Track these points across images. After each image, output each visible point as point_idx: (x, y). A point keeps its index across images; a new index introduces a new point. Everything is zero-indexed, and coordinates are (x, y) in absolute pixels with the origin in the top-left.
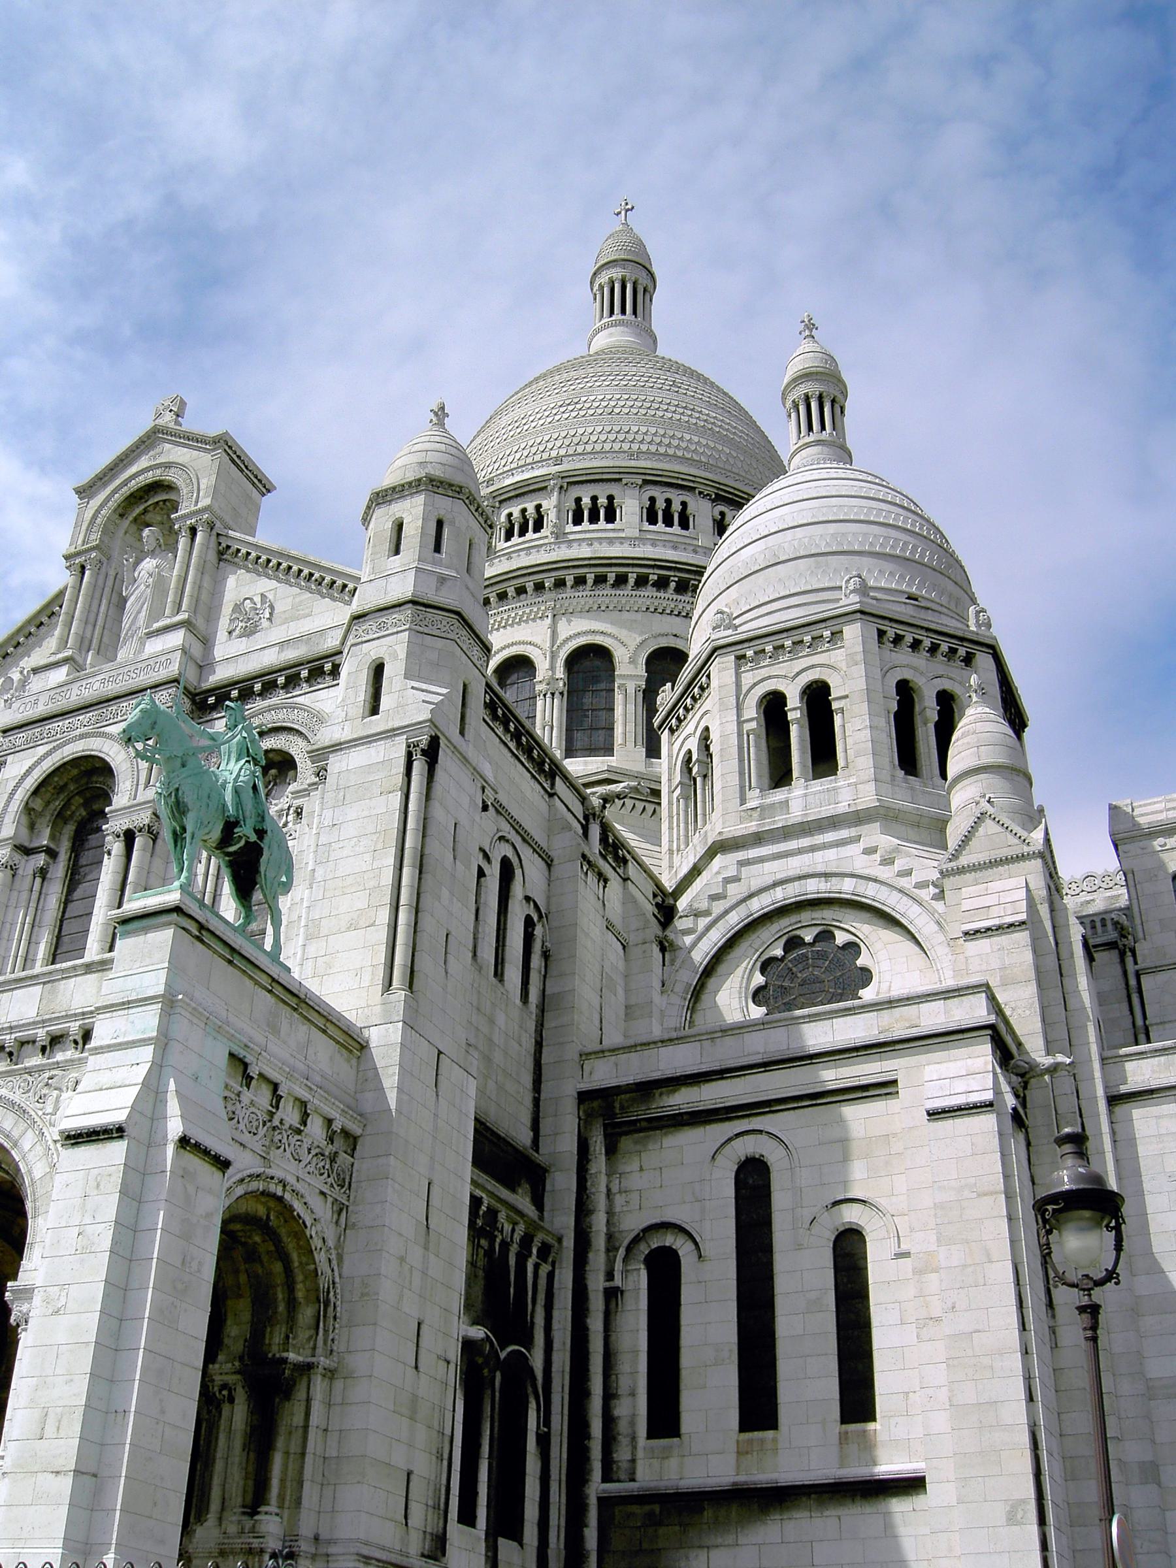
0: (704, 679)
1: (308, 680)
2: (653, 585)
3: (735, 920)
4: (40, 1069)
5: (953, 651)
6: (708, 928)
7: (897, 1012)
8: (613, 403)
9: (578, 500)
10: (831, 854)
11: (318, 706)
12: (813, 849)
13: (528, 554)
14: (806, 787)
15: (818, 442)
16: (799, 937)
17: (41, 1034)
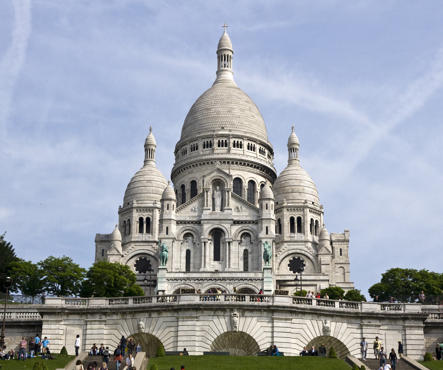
0: (280, 210)
1: (252, 223)
2: (250, 166)
3: (286, 254)
4: (256, 282)
5: (318, 213)
6: (282, 254)
7: (317, 276)
8: (239, 114)
9: (234, 141)
10: (301, 246)
11: (254, 228)
12: (298, 245)
13: (226, 155)
14: (297, 234)
15: (295, 159)
16: (295, 258)
17: (256, 279)
